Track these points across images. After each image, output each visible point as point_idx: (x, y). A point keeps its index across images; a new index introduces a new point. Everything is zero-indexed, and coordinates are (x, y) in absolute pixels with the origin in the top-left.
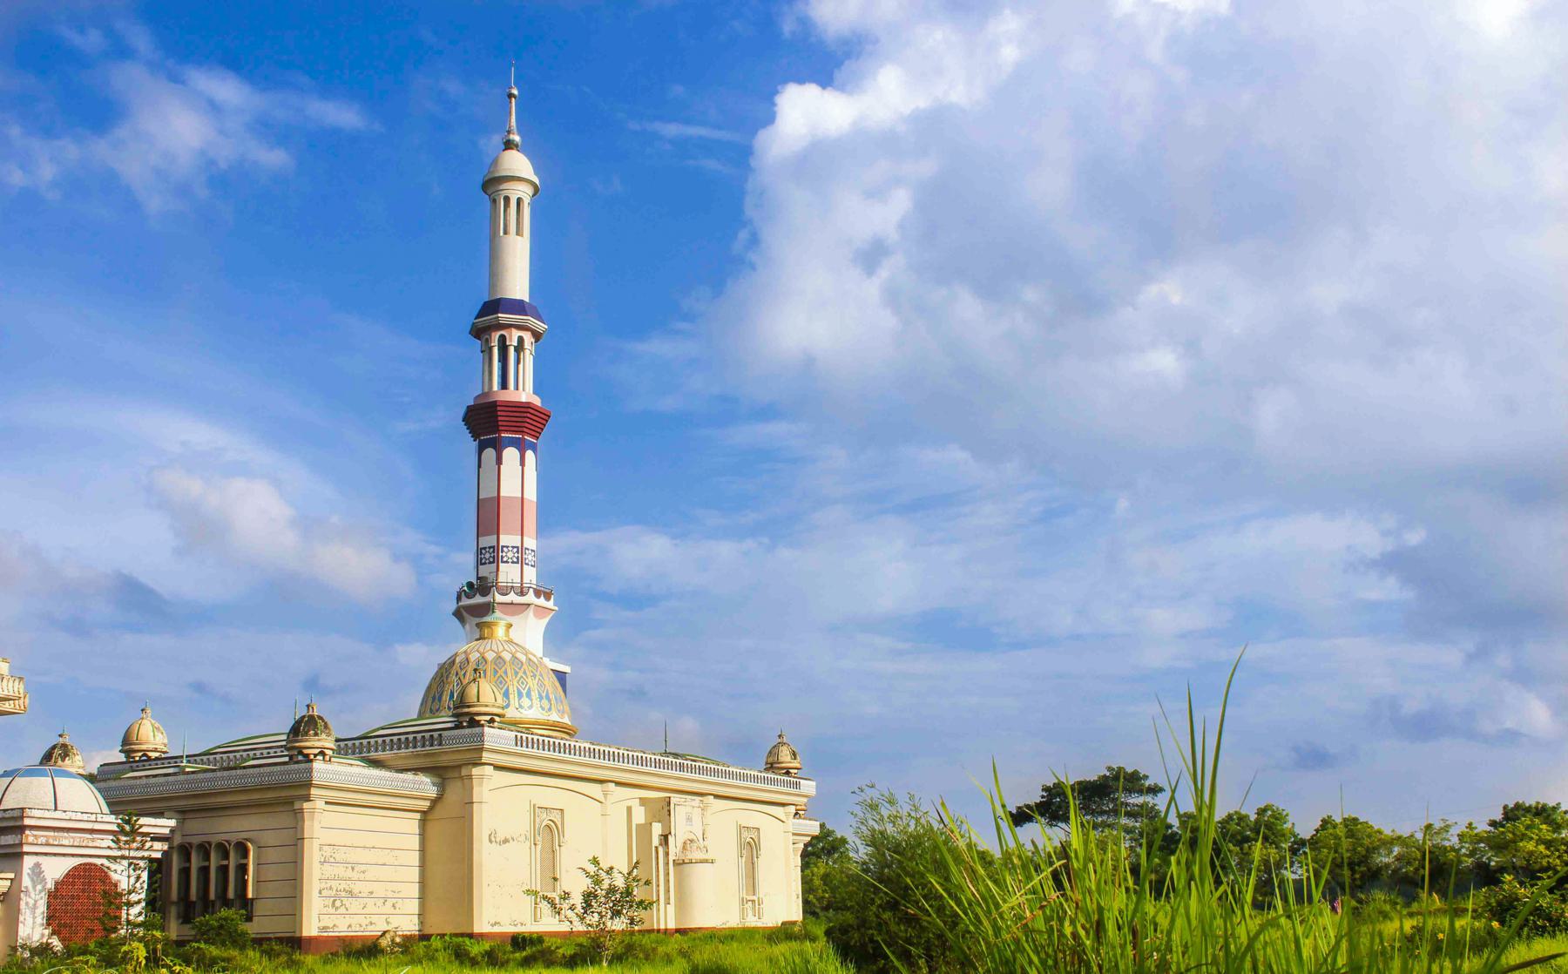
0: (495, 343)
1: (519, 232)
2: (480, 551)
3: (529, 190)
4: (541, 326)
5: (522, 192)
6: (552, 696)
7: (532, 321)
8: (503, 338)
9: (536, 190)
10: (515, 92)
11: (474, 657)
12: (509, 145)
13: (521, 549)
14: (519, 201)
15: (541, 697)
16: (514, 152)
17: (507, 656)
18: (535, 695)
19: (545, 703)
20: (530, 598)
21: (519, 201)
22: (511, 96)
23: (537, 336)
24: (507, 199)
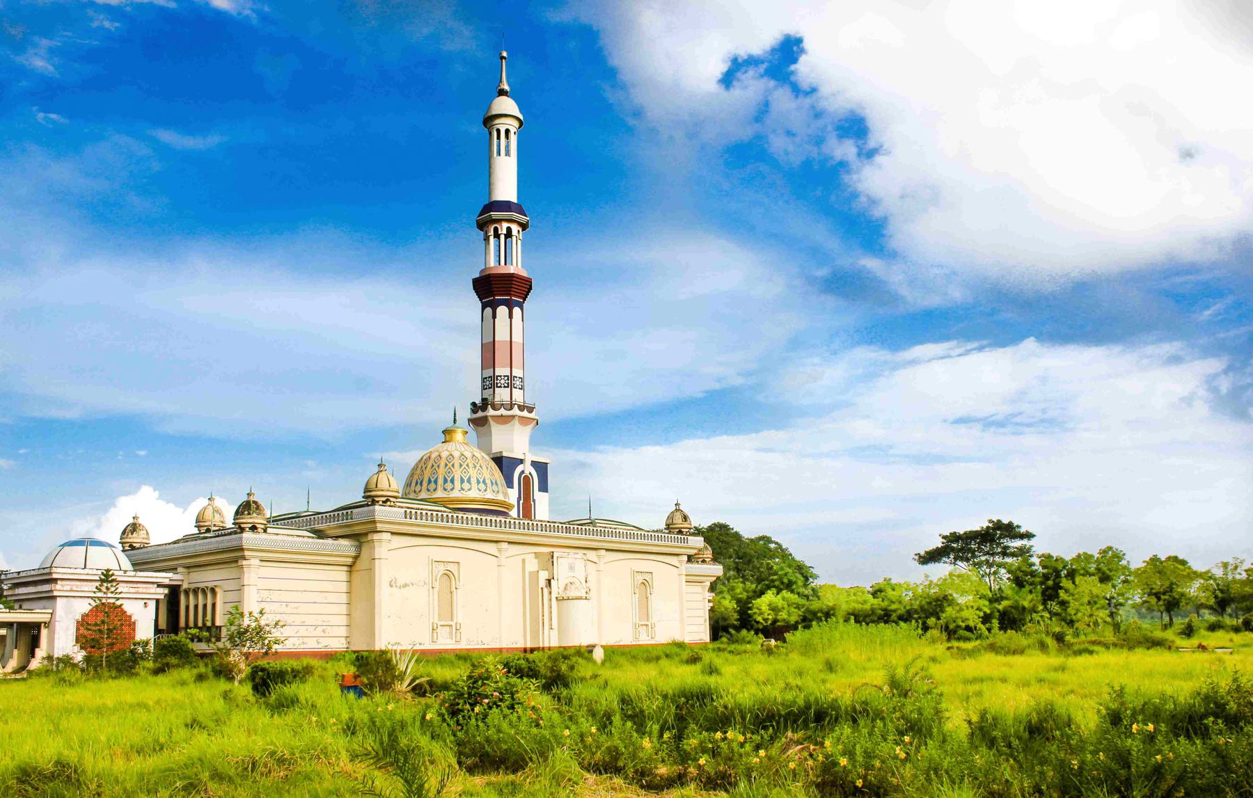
0: (492, 233)
1: (508, 154)
2: (484, 380)
3: (516, 124)
4: (523, 219)
5: (513, 125)
6: (488, 482)
7: (515, 215)
8: (496, 230)
9: (521, 123)
10: (505, 54)
11: (445, 454)
12: (502, 93)
13: (511, 378)
14: (507, 131)
15: (478, 482)
16: (504, 98)
17: (457, 454)
18: (474, 481)
19: (482, 486)
20: (516, 411)
21: (507, 131)
22: (502, 58)
23: (524, 226)
24: (498, 131)
